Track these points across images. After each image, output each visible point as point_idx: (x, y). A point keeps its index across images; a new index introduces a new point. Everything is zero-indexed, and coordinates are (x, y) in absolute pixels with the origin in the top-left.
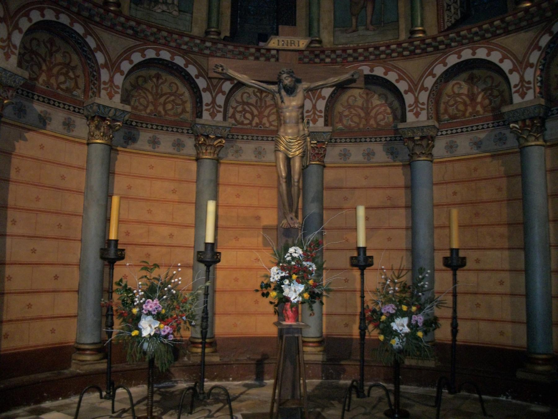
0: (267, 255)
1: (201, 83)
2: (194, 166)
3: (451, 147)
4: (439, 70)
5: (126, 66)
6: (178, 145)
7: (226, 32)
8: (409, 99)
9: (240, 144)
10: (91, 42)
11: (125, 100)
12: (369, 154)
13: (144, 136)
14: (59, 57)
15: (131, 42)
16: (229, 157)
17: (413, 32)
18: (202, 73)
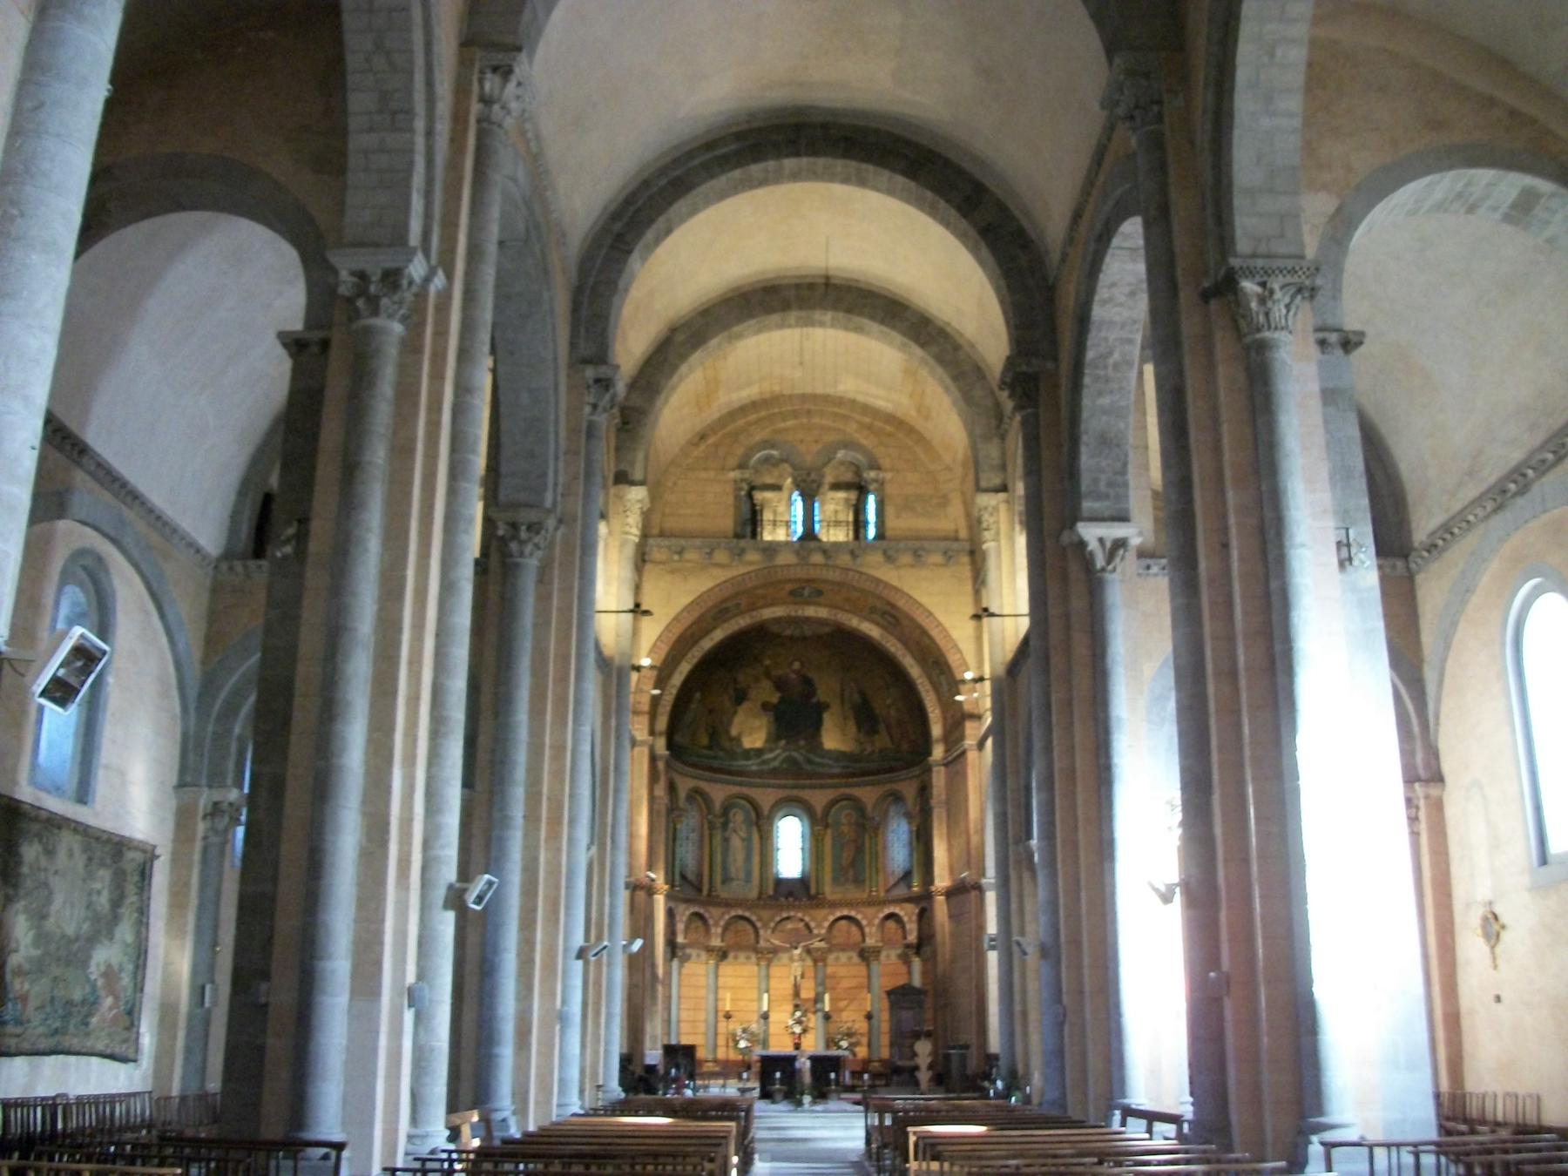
0: (788, 1015)
1: (759, 924)
2: (756, 968)
3: (888, 957)
4: (881, 915)
5: (722, 923)
6: (748, 958)
7: (771, 892)
8: (867, 930)
9: (781, 955)
10: (707, 915)
11: (722, 941)
12: (850, 958)
13: (731, 955)
14: (693, 925)
15: (721, 910)
16: (775, 962)
17: (871, 891)
18: (760, 919)
